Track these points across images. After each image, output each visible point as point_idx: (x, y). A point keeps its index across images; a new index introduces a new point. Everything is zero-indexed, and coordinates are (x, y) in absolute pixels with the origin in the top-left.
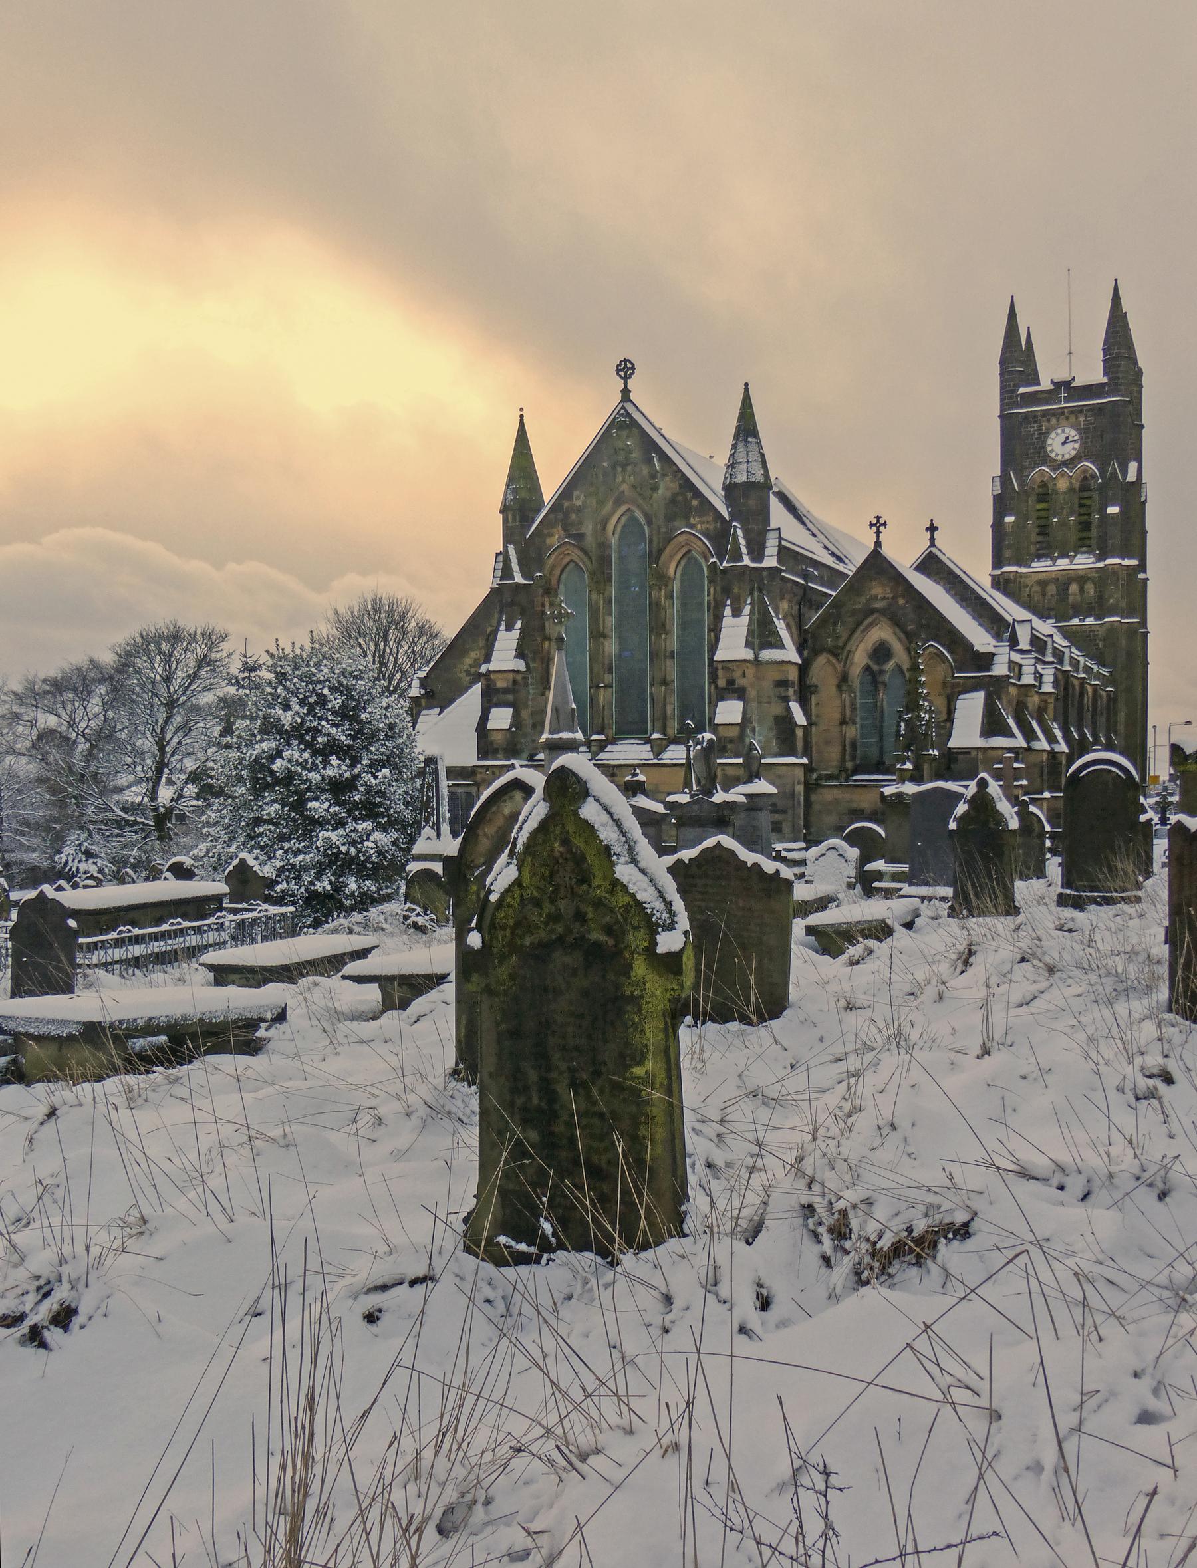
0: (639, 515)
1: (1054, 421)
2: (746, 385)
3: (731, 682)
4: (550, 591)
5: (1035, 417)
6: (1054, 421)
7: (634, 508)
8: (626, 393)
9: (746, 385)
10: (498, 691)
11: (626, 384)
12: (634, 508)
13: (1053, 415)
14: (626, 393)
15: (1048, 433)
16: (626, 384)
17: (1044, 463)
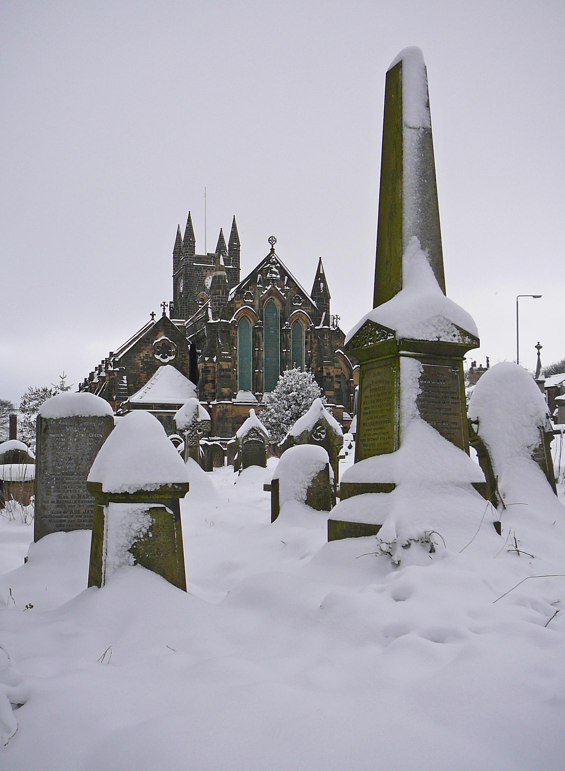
0: (277, 302)
1: (208, 272)
2: (320, 258)
3: (328, 374)
4: (236, 328)
5: (201, 268)
6: (208, 272)
7: (274, 298)
8: (272, 250)
9: (320, 258)
10: (223, 370)
11: (272, 246)
12: (274, 298)
13: (209, 269)
14: (272, 250)
15: (205, 277)
16: (272, 246)
17: (204, 291)
